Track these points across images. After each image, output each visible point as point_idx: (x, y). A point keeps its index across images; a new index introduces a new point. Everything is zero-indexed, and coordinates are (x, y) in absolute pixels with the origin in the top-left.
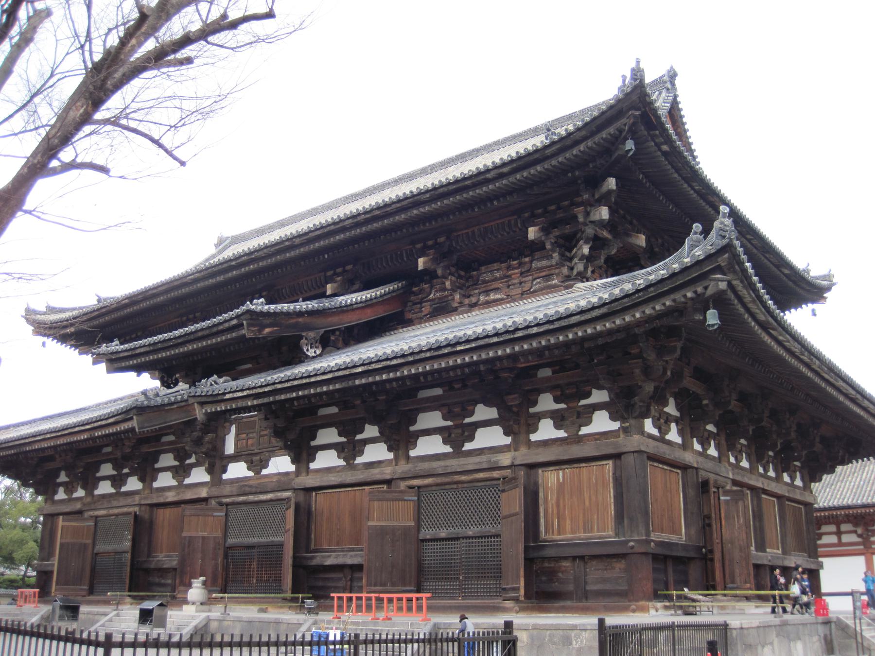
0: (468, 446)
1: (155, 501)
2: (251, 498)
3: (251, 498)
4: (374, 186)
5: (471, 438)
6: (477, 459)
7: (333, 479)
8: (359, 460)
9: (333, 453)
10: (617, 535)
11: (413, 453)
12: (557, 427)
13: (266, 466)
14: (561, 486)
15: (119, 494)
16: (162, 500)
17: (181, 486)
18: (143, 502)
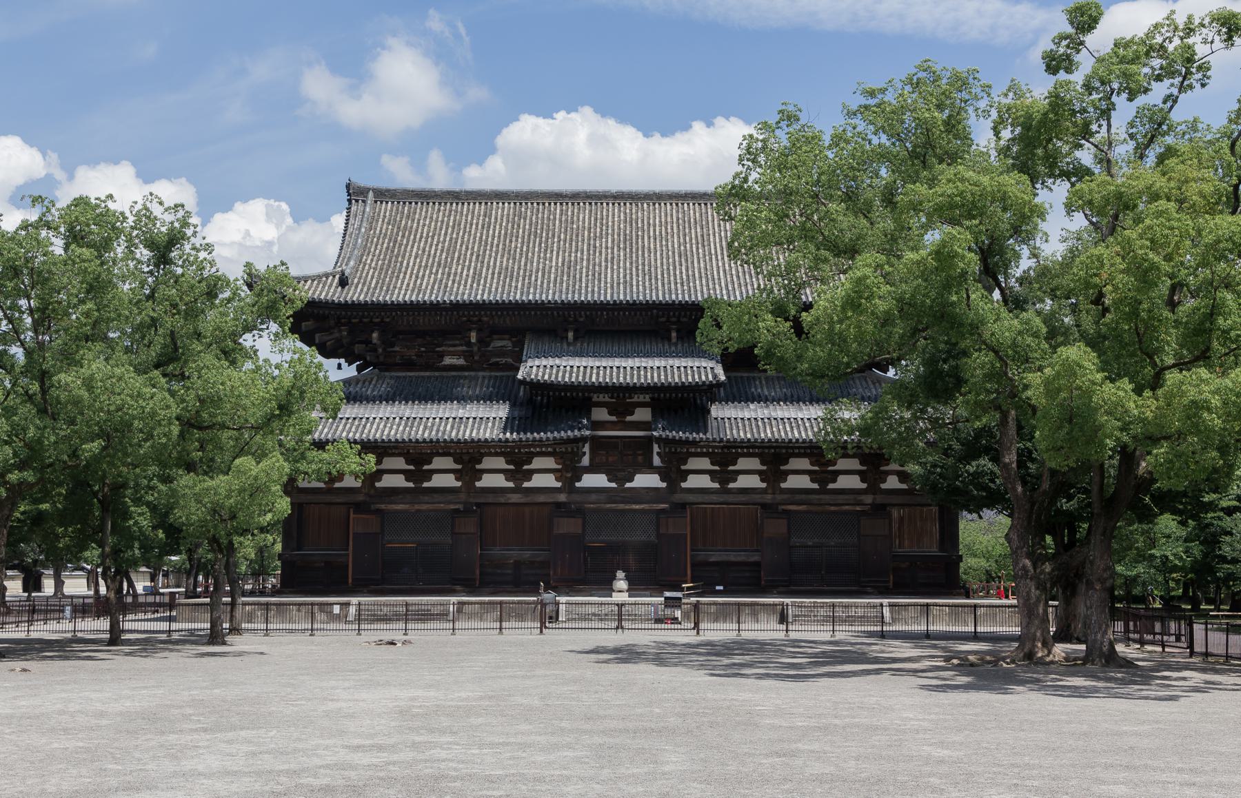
0: (831, 486)
1: (482, 501)
2: (621, 506)
3: (621, 506)
4: (586, 193)
5: (834, 481)
6: (846, 497)
7: (707, 498)
8: (731, 485)
9: (707, 477)
10: (940, 551)
11: (783, 485)
12: (901, 481)
13: (631, 480)
14: (901, 519)
15: (419, 492)
16: (502, 500)
17: (518, 490)
18: (472, 500)
